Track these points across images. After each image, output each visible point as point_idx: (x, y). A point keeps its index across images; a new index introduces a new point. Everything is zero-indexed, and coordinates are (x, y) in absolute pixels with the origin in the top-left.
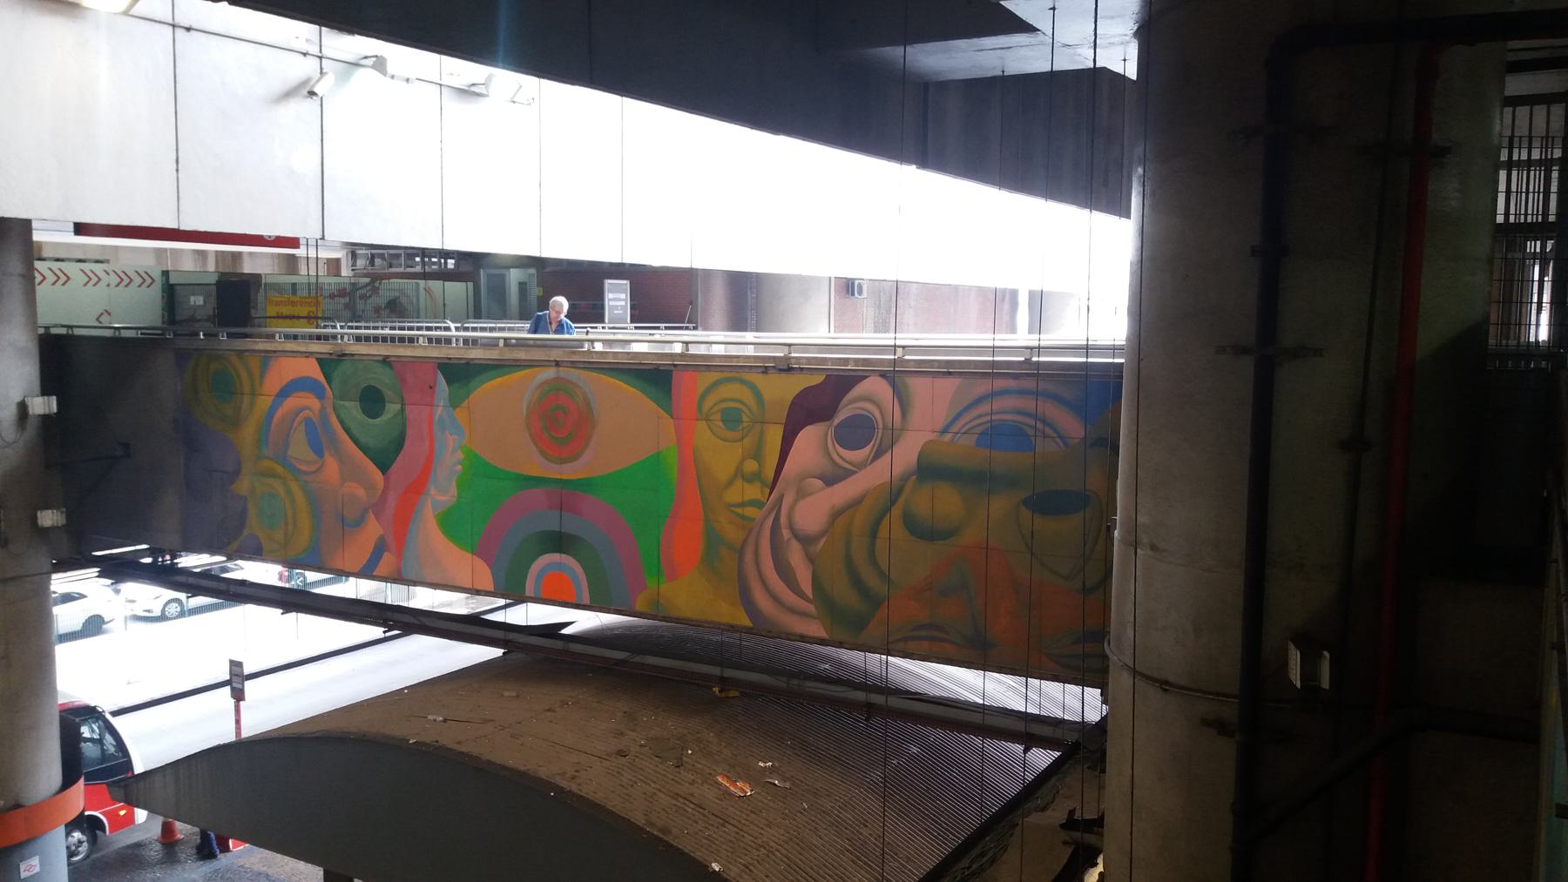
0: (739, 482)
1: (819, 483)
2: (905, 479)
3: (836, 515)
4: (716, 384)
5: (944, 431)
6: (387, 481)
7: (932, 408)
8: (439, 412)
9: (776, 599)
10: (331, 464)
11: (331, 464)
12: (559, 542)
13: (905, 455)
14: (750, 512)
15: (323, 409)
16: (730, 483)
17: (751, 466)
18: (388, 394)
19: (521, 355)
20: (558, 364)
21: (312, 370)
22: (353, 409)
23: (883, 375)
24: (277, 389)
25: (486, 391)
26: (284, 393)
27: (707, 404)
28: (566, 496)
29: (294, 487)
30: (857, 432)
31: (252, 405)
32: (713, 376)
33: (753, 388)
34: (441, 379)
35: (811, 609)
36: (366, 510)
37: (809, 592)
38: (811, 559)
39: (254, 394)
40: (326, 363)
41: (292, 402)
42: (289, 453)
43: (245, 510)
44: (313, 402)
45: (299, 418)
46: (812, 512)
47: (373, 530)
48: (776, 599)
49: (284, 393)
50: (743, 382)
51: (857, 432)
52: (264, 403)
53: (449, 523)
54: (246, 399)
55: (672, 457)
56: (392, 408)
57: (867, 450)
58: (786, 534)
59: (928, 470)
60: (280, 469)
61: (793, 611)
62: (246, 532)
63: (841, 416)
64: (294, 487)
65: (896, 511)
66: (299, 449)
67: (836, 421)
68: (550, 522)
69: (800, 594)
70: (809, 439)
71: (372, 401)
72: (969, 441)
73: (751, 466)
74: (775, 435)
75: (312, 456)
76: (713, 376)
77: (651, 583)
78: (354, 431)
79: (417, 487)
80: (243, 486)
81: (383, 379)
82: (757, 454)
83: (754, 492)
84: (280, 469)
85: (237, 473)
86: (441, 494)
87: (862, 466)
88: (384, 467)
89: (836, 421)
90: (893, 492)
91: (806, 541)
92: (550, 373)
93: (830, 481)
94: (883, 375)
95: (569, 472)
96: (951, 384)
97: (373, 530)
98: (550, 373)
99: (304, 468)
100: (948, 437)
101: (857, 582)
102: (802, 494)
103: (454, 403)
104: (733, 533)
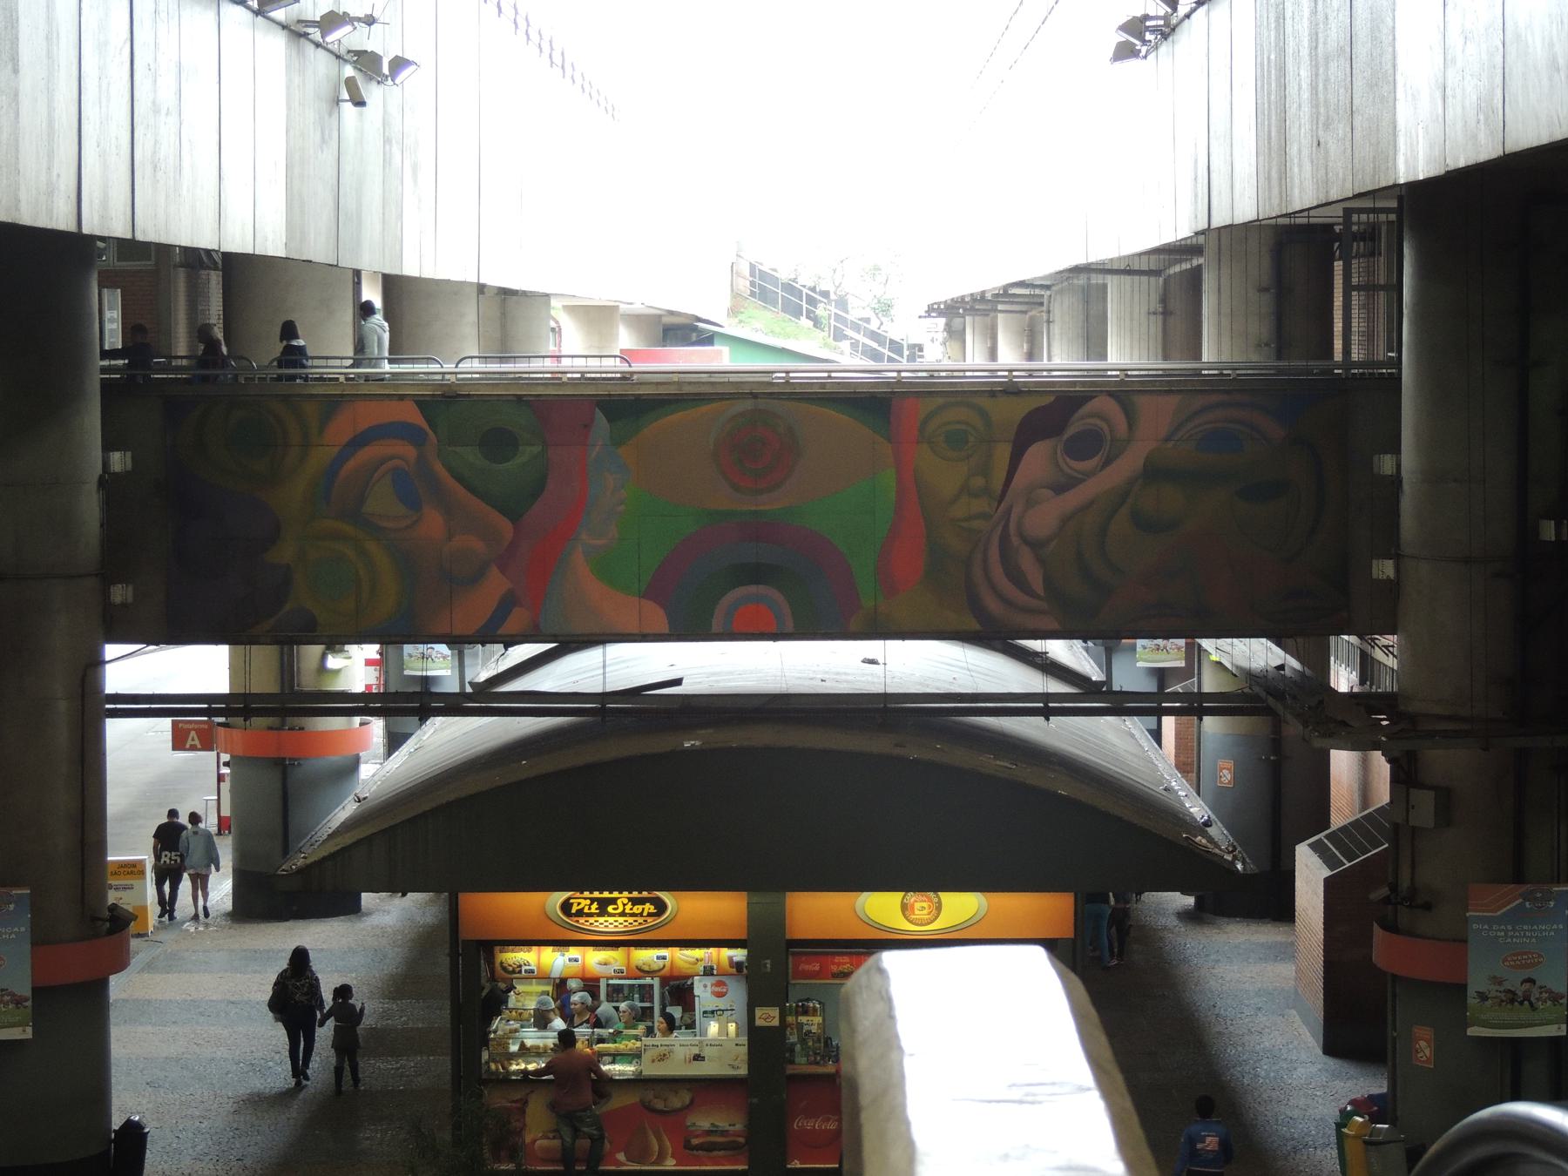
1: (1049, 493)
3: (1065, 520)
5: (1167, 439)
7: (1156, 419)
9: (1008, 603)
10: (433, 522)
12: (756, 574)
13: (1129, 464)
14: (976, 524)
17: (978, 482)
22: (471, 456)
23: (1110, 394)
24: (346, 439)
30: (1087, 445)
32: (940, 401)
34: (600, 418)
37: (1041, 592)
40: (423, 404)
41: (365, 454)
44: (409, 451)
45: (390, 464)
46: (1044, 518)
47: (496, 585)
51: (1087, 445)
52: (321, 456)
56: (527, 452)
57: (1096, 459)
58: (1015, 541)
59: (1154, 472)
62: (288, 607)
63: (1071, 431)
66: (382, 502)
67: (1066, 437)
70: (1039, 456)
73: (978, 482)
74: (1003, 452)
80: (285, 553)
88: (514, 515)
89: (1066, 437)
91: (1035, 545)
93: (1060, 489)
94: (1110, 394)
96: (1174, 400)
97: (496, 585)
98: (748, 404)
100: (1170, 444)
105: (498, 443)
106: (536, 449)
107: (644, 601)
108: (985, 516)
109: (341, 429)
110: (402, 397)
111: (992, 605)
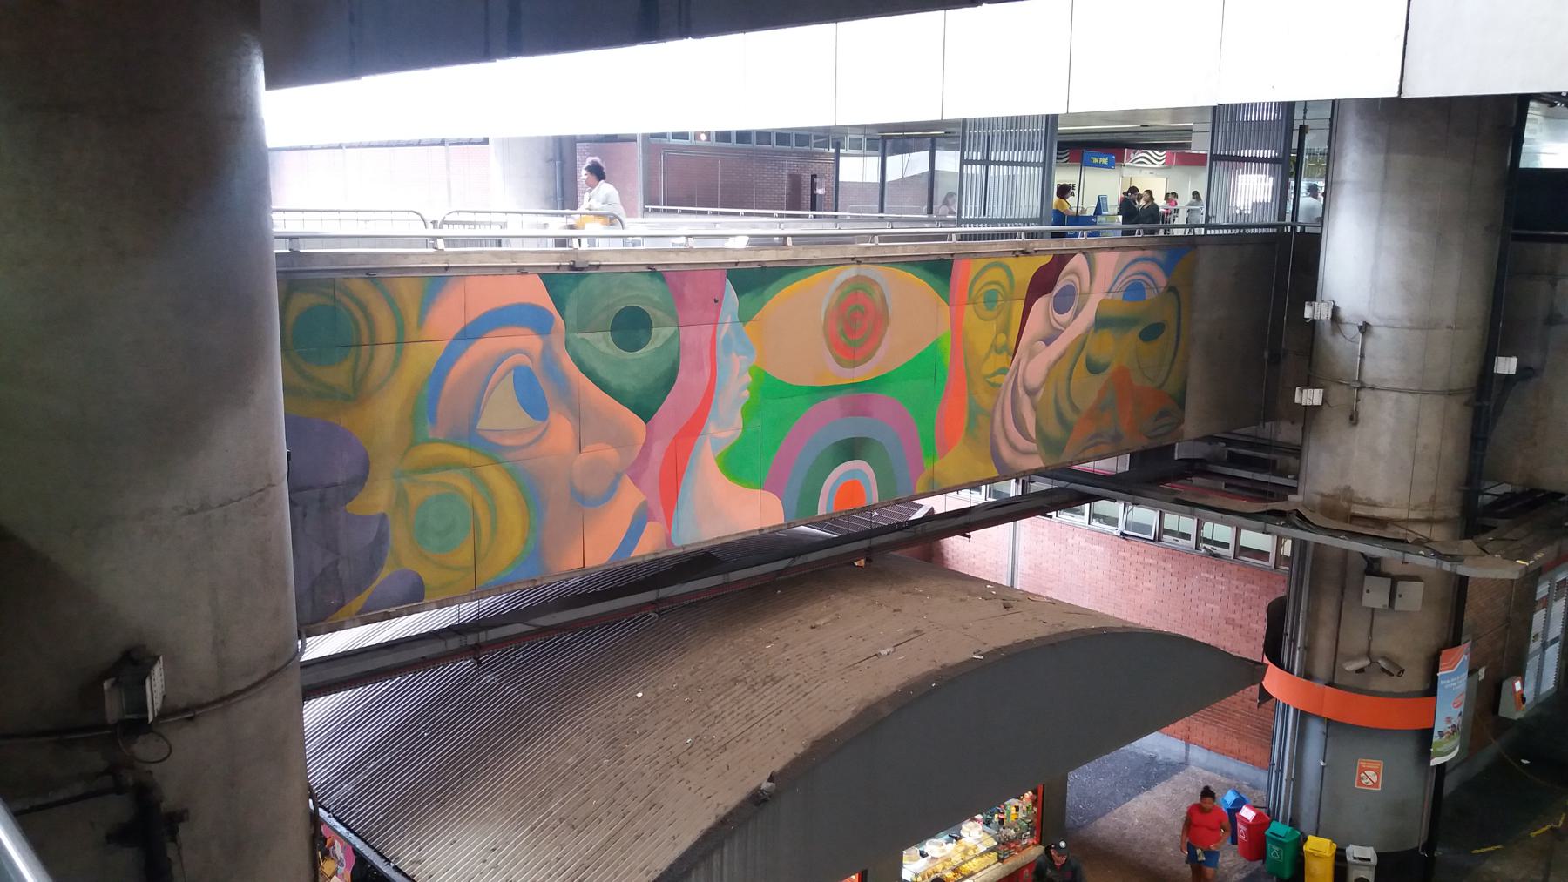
0: (993, 354)
2: (1087, 331)
4: (986, 268)
6: (649, 431)
8: (724, 330)
9: (1014, 448)
10: (561, 430)
11: (561, 430)
12: (851, 449)
14: (998, 379)
15: (547, 348)
16: (987, 356)
17: (1002, 338)
18: (656, 314)
19: (815, 253)
20: (857, 261)
21: (536, 293)
22: (601, 343)
24: (455, 329)
25: (782, 298)
26: (469, 334)
27: (977, 287)
28: (858, 398)
29: (493, 475)
31: (397, 363)
33: (1007, 269)
35: (1033, 447)
36: (618, 476)
37: (1033, 434)
38: (1035, 408)
39: (401, 341)
40: (552, 280)
42: (483, 424)
43: (381, 539)
44: (533, 342)
48: (1014, 448)
49: (469, 334)
50: (1000, 265)
52: (422, 356)
53: (734, 464)
54: (384, 354)
55: (946, 345)
56: (660, 335)
58: (1021, 391)
59: (1101, 323)
60: (462, 454)
61: (1026, 453)
62: (384, 574)
64: (493, 475)
65: (1083, 355)
66: (502, 414)
68: (849, 429)
69: (1026, 436)
71: (631, 326)
72: (1119, 296)
73: (1002, 338)
75: (525, 420)
76: (982, 263)
77: (928, 465)
78: (602, 371)
79: (694, 427)
80: (377, 498)
81: (649, 296)
82: (1005, 330)
83: (1001, 361)
84: (462, 454)
85: (360, 480)
86: (724, 428)
87: (1065, 326)
88: (646, 414)
90: (1082, 342)
91: (1031, 393)
92: (851, 271)
93: (1048, 341)
95: (861, 374)
98: (851, 271)
99: (508, 442)
101: (1060, 416)
102: (1032, 354)
103: (744, 317)
104: (985, 399)
105: (631, 326)
106: (668, 331)
107: (766, 494)
108: (1003, 371)
109: (447, 316)
110: (522, 270)
111: (1006, 452)
